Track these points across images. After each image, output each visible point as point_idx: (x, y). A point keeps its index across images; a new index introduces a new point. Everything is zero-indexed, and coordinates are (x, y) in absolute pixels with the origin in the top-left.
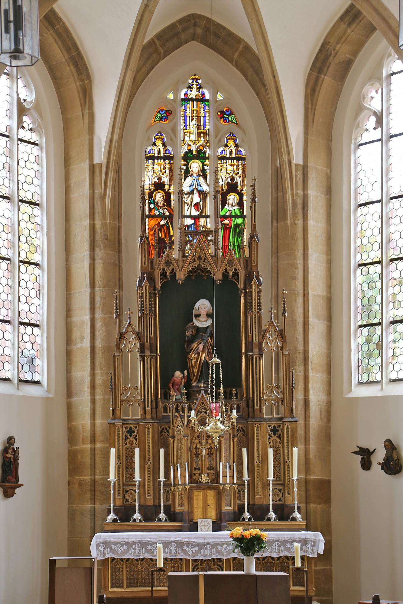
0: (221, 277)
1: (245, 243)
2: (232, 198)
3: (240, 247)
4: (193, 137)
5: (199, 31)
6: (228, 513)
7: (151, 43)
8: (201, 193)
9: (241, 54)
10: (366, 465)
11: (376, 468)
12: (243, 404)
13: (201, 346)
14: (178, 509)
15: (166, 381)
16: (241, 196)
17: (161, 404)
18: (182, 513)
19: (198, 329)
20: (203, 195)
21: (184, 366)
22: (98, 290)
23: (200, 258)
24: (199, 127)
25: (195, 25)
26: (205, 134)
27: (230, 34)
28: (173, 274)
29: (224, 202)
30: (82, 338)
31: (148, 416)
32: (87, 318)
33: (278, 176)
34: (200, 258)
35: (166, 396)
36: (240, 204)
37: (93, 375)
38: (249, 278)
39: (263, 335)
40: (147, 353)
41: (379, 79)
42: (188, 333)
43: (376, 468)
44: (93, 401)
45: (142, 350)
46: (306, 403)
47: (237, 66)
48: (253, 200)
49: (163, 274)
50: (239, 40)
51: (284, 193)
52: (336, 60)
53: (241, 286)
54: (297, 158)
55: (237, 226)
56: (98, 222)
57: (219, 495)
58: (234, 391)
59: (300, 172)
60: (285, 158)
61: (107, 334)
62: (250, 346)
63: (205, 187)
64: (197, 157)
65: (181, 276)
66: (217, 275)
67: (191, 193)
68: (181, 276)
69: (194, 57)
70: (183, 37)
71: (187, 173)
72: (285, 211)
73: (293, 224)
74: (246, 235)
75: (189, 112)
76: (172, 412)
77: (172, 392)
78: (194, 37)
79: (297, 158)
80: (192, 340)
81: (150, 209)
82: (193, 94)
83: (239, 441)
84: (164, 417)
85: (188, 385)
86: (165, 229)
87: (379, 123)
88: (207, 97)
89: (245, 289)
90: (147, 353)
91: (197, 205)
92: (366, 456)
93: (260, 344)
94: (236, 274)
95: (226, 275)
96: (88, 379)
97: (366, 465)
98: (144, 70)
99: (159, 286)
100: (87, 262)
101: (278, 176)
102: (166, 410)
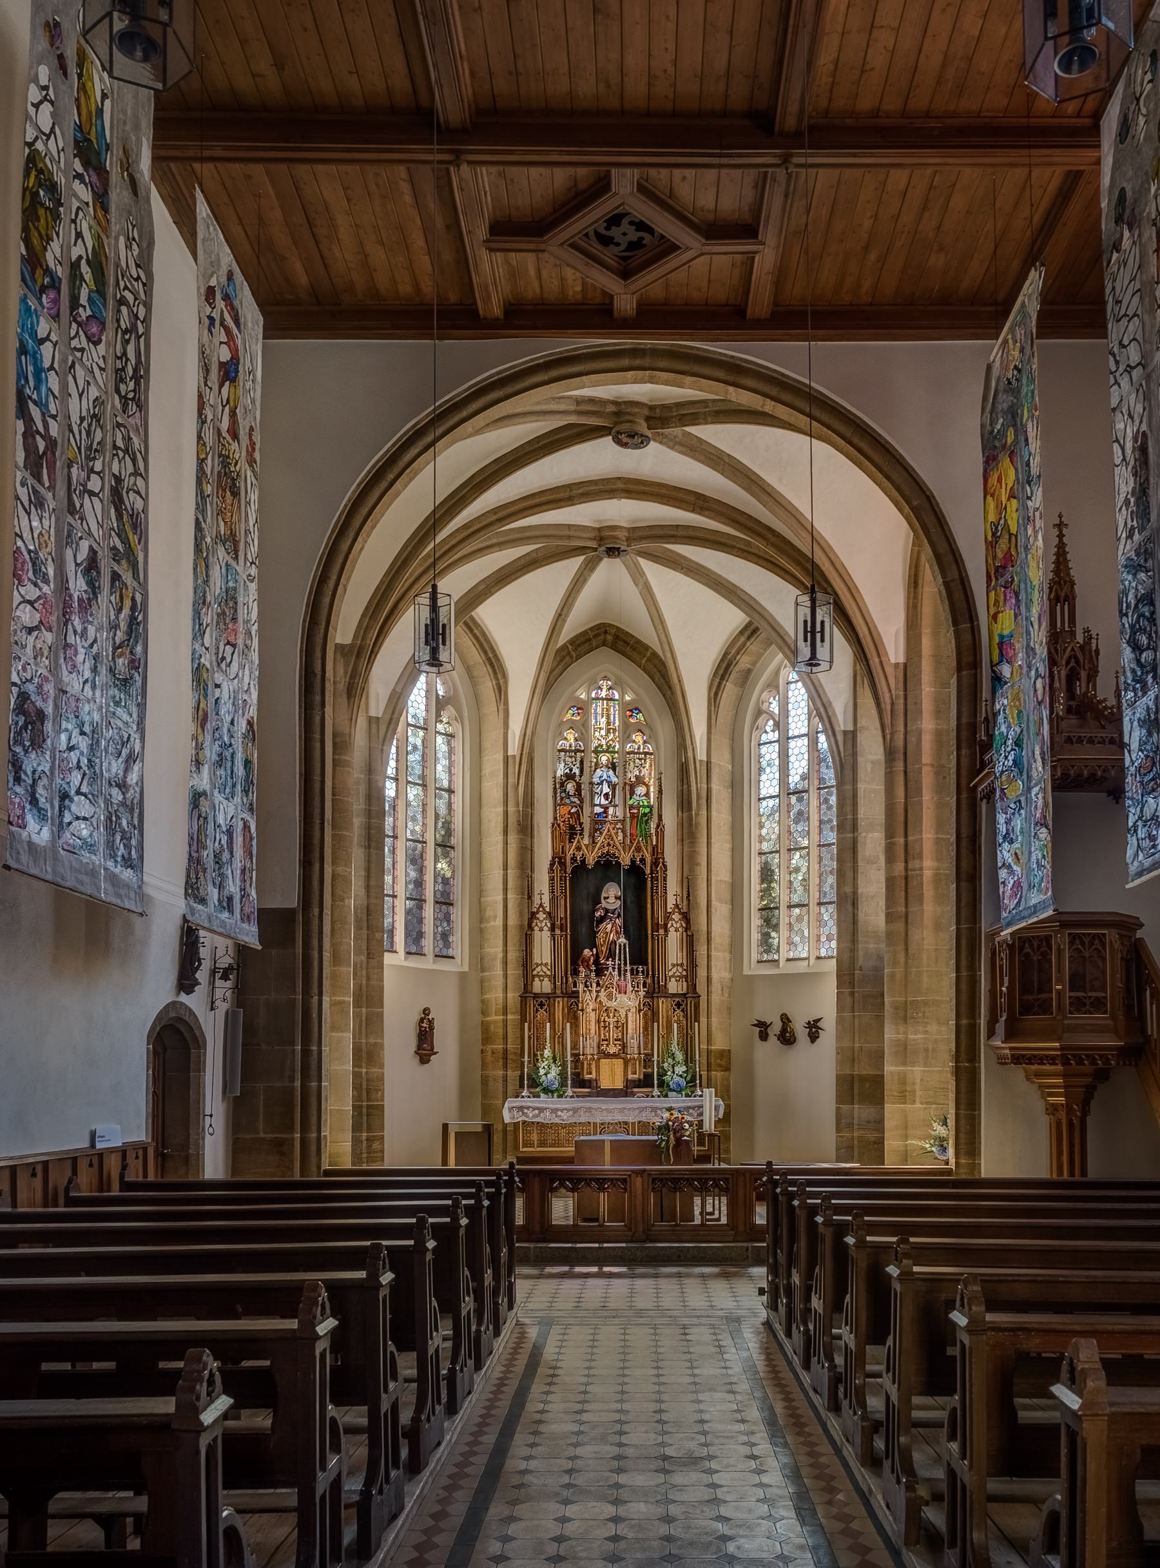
0: (628, 862)
1: (653, 831)
2: (641, 790)
3: (647, 836)
4: (603, 732)
5: (609, 638)
6: (634, 1081)
7: (564, 647)
8: (609, 783)
9: (649, 660)
10: (764, 1036)
11: (773, 1039)
12: (649, 981)
13: (609, 926)
14: (587, 1077)
15: (576, 959)
16: (648, 786)
17: (570, 979)
18: (590, 1081)
19: (607, 911)
20: (613, 787)
21: (593, 945)
22: (511, 873)
23: (609, 845)
24: (608, 723)
25: (606, 632)
26: (614, 730)
27: (638, 641)
28: (583, 861)
29: (632, 793)
30: (495, 917)
31: (558, 992)
32: (500, 898)
33: (683, 772)
34: (609, 845)
35: (576, 973)
36: (647, 795)
37: (506, 951)
38: (655, 863)
39: (668, 917)
40: (558, 932)
41: (777, 688)
42: (597, 914)
43: (773, 1039)
44: (506, 976)
45: (552, 929)
46: (709, 979)
47: (644, 670)
48: (660, 792)
49: (574, 859)
50: (647, 648)
51: (689, 786)
52: (737, 669)
53: (648, 871)
54: (701, 755)
55: (645, 815)
56: (511, 809)
57: (626, 1062)
58: (640, 969)
59: (704, 767)
60: (690, 754)
61: (521, 913)
62: (656, 927)
63: (614, 780)
64: (607, 751)
65: (591, 861)
66: (625, 860)
67: (602, 783)
68: (591, 861)
69: (605, 660)
70: (594, 643)
71: (597, 766)
72: (690, 803)
73: (697, 815)
74: (653, 825)
75: (599, 710)
76: (581, 988)
77: (581, 969)
78: (604, 644)
79: (701, 755)
80: (602, 919)
81: (562, 799)
82: (603, 694)
83: (645, 1015)
84: (574, 992)
85: (596, 962)
86: (577, 816)
87: (777, 725)
88: (617, 697)
89: (652, 873)
90: (558, 932)
91: (606, 795)
92: (763, 1029)
93: (666, 925)
94: (643, 860)
95: (633, 862)
96: (500, 955)
97: (764, 1036)
98: (557, 671)
99: (569, 870)
100: (500, 846)
101: (683, 772)
102: (575, 986)
